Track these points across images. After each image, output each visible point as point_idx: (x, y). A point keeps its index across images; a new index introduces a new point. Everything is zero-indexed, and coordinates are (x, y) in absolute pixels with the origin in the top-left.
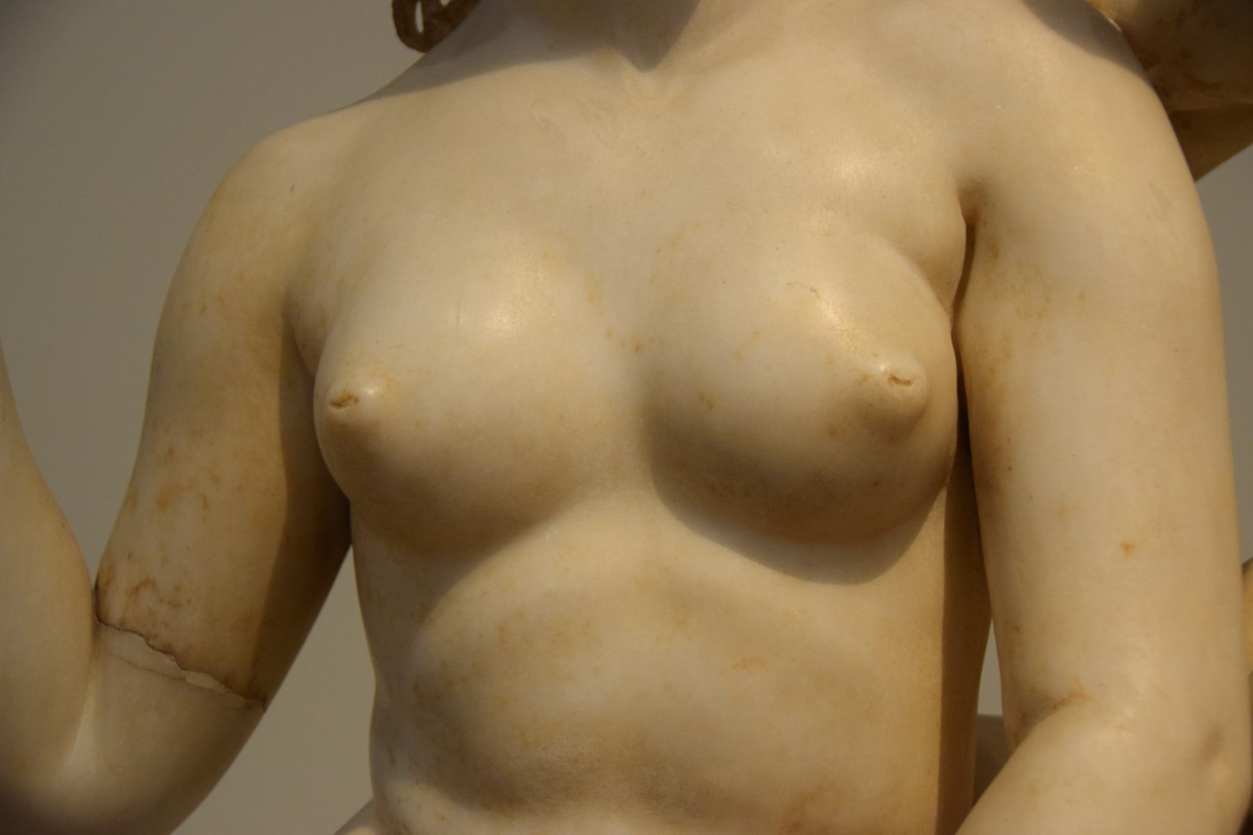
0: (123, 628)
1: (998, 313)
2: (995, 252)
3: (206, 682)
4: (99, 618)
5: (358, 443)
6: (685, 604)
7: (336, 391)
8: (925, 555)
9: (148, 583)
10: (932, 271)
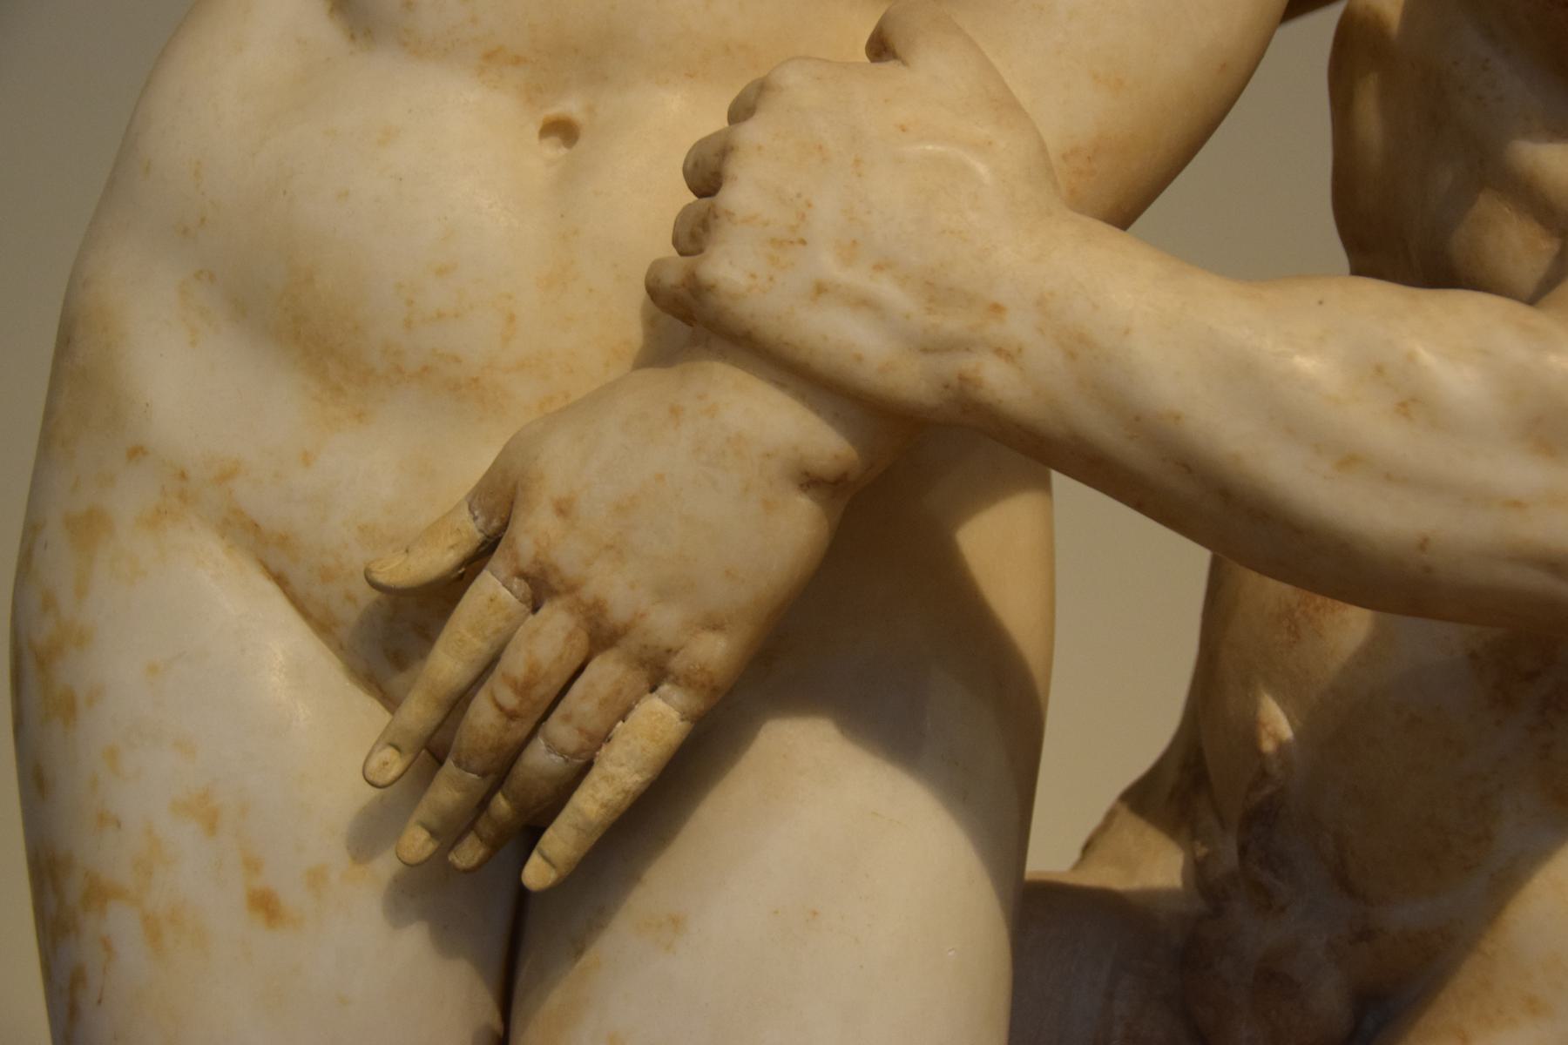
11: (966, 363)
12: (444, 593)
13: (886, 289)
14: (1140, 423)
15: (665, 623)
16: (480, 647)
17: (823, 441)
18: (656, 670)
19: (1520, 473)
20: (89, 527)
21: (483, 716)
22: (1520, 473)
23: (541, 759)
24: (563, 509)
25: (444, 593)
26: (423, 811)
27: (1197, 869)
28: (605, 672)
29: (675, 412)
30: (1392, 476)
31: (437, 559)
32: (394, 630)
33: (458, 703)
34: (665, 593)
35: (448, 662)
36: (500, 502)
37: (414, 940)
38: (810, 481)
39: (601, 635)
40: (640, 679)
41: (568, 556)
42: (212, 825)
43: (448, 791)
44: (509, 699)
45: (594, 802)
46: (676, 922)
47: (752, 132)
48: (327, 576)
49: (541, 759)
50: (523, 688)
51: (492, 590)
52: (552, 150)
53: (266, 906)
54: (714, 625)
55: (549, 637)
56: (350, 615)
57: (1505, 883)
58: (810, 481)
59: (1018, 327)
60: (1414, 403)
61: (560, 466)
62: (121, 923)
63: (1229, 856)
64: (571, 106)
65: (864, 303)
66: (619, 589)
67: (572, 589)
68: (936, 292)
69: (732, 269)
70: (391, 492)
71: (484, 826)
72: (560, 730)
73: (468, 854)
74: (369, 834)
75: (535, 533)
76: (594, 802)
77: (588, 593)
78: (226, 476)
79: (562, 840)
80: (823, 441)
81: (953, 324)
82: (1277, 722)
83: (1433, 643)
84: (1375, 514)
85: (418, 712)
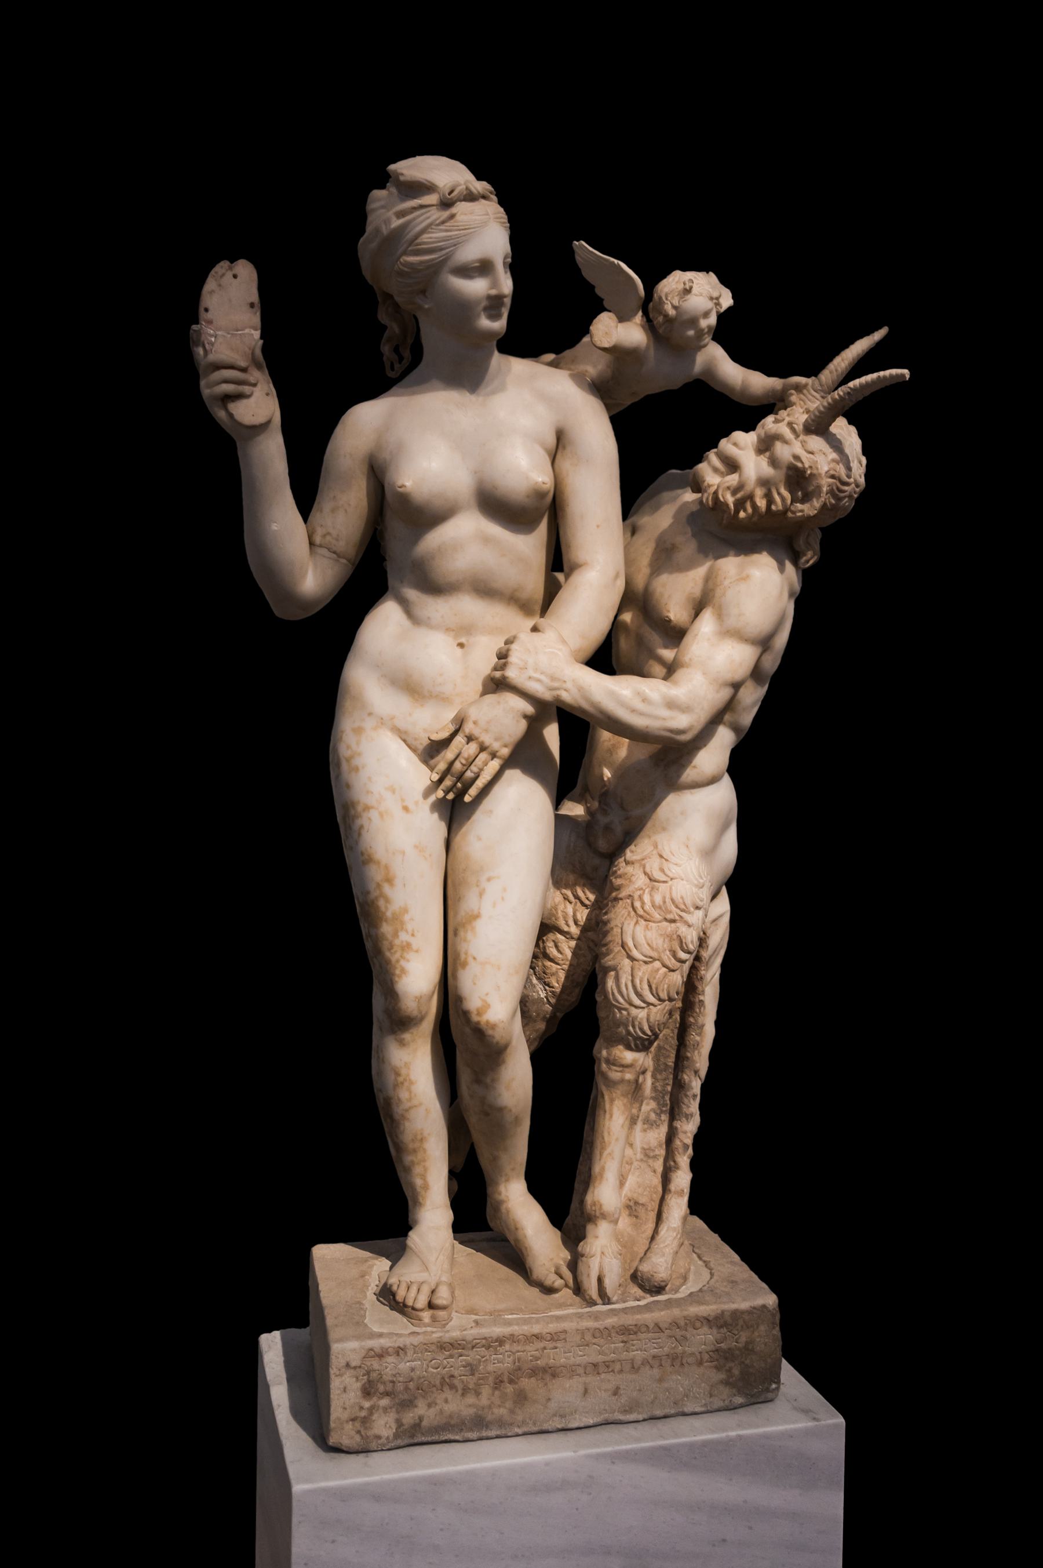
0: (321, 546)
1: (565, 464)
2: (564, 448)
3: (344, 561)
4: (311, 544)
5: (404, 499)
6: (487, 540)
7: (400, 483)
8: (543, 527)
9: (329, 534)
10: (549, 455)
11: (558, 692)
12: (446, 743)
13: (543, 677)
14: (593, 704)
15: (496, 746)
16: (457, 751)
17: (530, 709)
18: (494, 755)
19: (664, 713)
20: (359, 731)
21: (458, 766)
22: (664, 713)
23: (469, 774)
24: (475, 723)
25: (446, 743)
26: (442, 786)
27: (588, 811)
28: (483, 756)
29: (499, 703)
30: (642, 714)
31: (445, 735)
32: (432, 751)
33: (451, 764)
34: (496, 739)
35: (449, 754)
37: (436, 815)
38: (525, 717)
39: (483, 748)
40: (490, 757)
41: (476, 732)
42: (394, 792)
43: (448, 782)
44: (464, 762)
45: (480, 783)
46: (491, 812)
47: (514, 647)
48: (416, 739)
49: (469, 774)
50: (466, 759)
51: (459, 739)
52: (459, 650)
53: (406, 809)
54: (506, 746)
56: (421, 748)
57: (657, 804)
58: (525, 717)
59: (569, 685)
60: (644, 700)
61: (473, 713)
62: (374, 814)
63: (596, 804)
64: (463, 640)
65: (539, 680)
66: (487, 739)
67: (477, 739)
68: (553, 678)
69: (512, 674)
70: (432, 721)
71: (454, 790)
72: (474, 768)
73: (451, 796)
74: (427, 794)
75: (468, 728)
76: (480, 783)
77: (481, 739)
78: (392, 718)
79: (473, 791)
80: (530, 709)
81: (556, 684)
82: (607, 774)
83: (643, 752)
84: (638, 721)
85: (442, 766)
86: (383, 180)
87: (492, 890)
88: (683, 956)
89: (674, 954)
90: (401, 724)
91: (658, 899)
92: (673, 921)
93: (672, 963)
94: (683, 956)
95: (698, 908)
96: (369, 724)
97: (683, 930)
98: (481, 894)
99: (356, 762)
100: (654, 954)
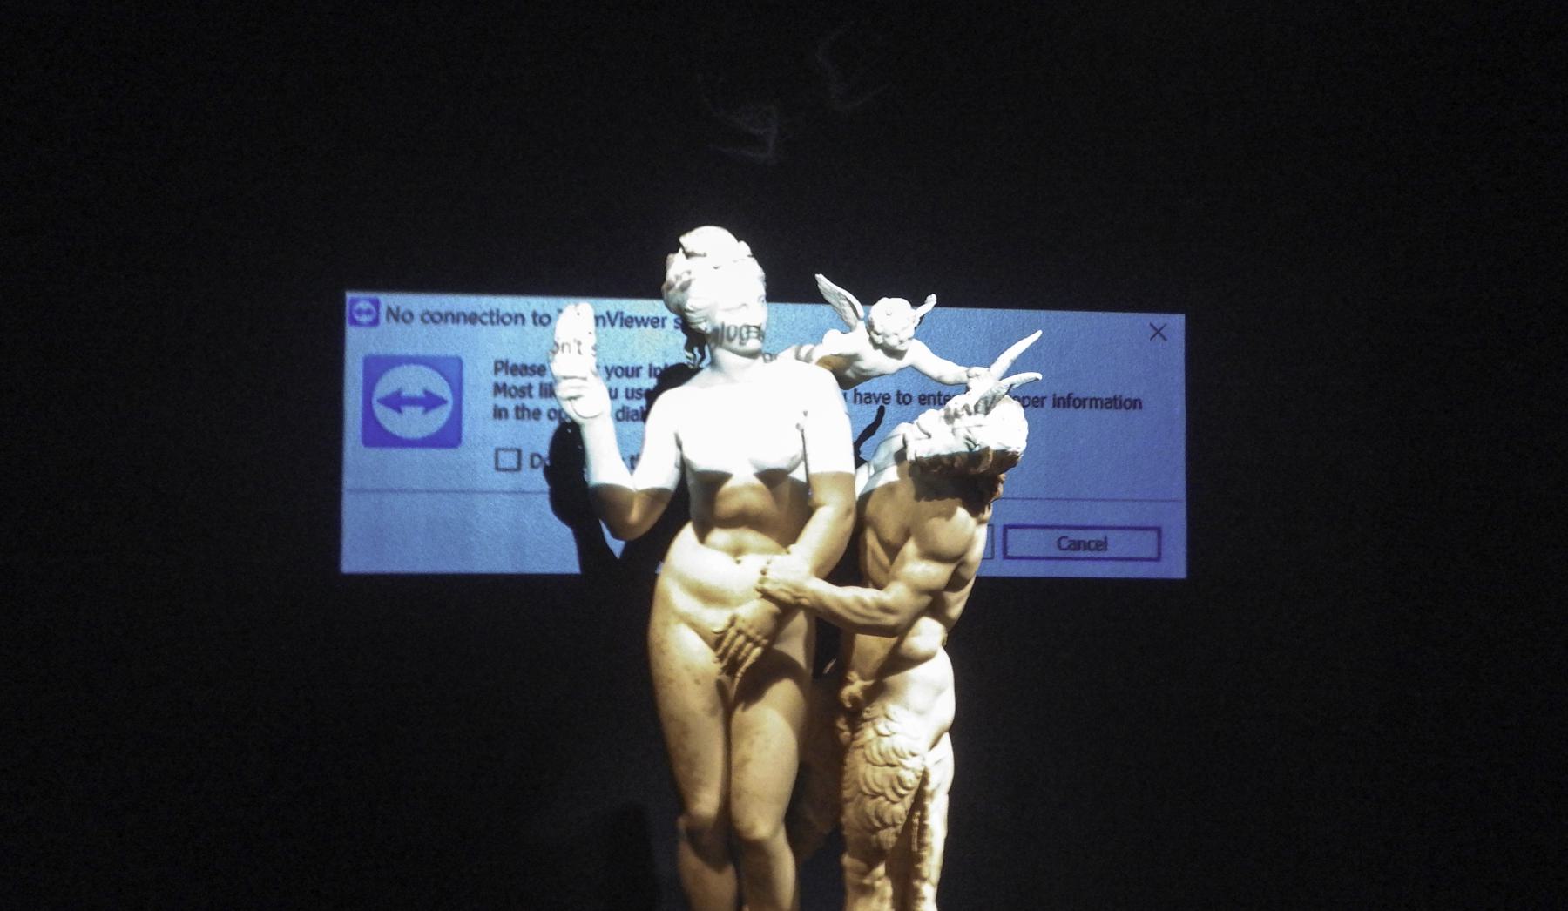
15: (759, 637)
18: (757, 644)
19: (877, 614)
20: (666, 624)
21: (731, 651)
22: (877, 614)
28: (749, 645)
30: (862, 616)
33: (726, 650)
35: (725, 644)
36: (732, 622)
39: (749, 639)
55: (741, 639)
66: (751, 632)
68: (797, 589)
70: (716, 619)
76: (747, 664)
85: (720, 651)
86: (676, 247)
87: (759, 741)
88: (902, 791)
89: (894, 789)
90: (694, 619)
91: (883, 748)
92: (893, 766)
93: (893, 796)
94: (902, 791)
95: (914, 755)
96: (673, 620)
97: (902, 772)
98: (751, 743)
99: (664, 647)
100: (878, 790)
